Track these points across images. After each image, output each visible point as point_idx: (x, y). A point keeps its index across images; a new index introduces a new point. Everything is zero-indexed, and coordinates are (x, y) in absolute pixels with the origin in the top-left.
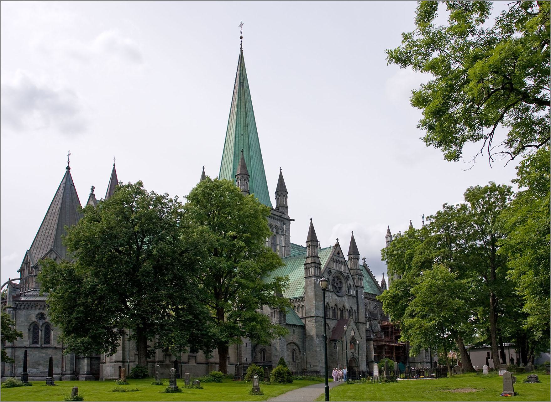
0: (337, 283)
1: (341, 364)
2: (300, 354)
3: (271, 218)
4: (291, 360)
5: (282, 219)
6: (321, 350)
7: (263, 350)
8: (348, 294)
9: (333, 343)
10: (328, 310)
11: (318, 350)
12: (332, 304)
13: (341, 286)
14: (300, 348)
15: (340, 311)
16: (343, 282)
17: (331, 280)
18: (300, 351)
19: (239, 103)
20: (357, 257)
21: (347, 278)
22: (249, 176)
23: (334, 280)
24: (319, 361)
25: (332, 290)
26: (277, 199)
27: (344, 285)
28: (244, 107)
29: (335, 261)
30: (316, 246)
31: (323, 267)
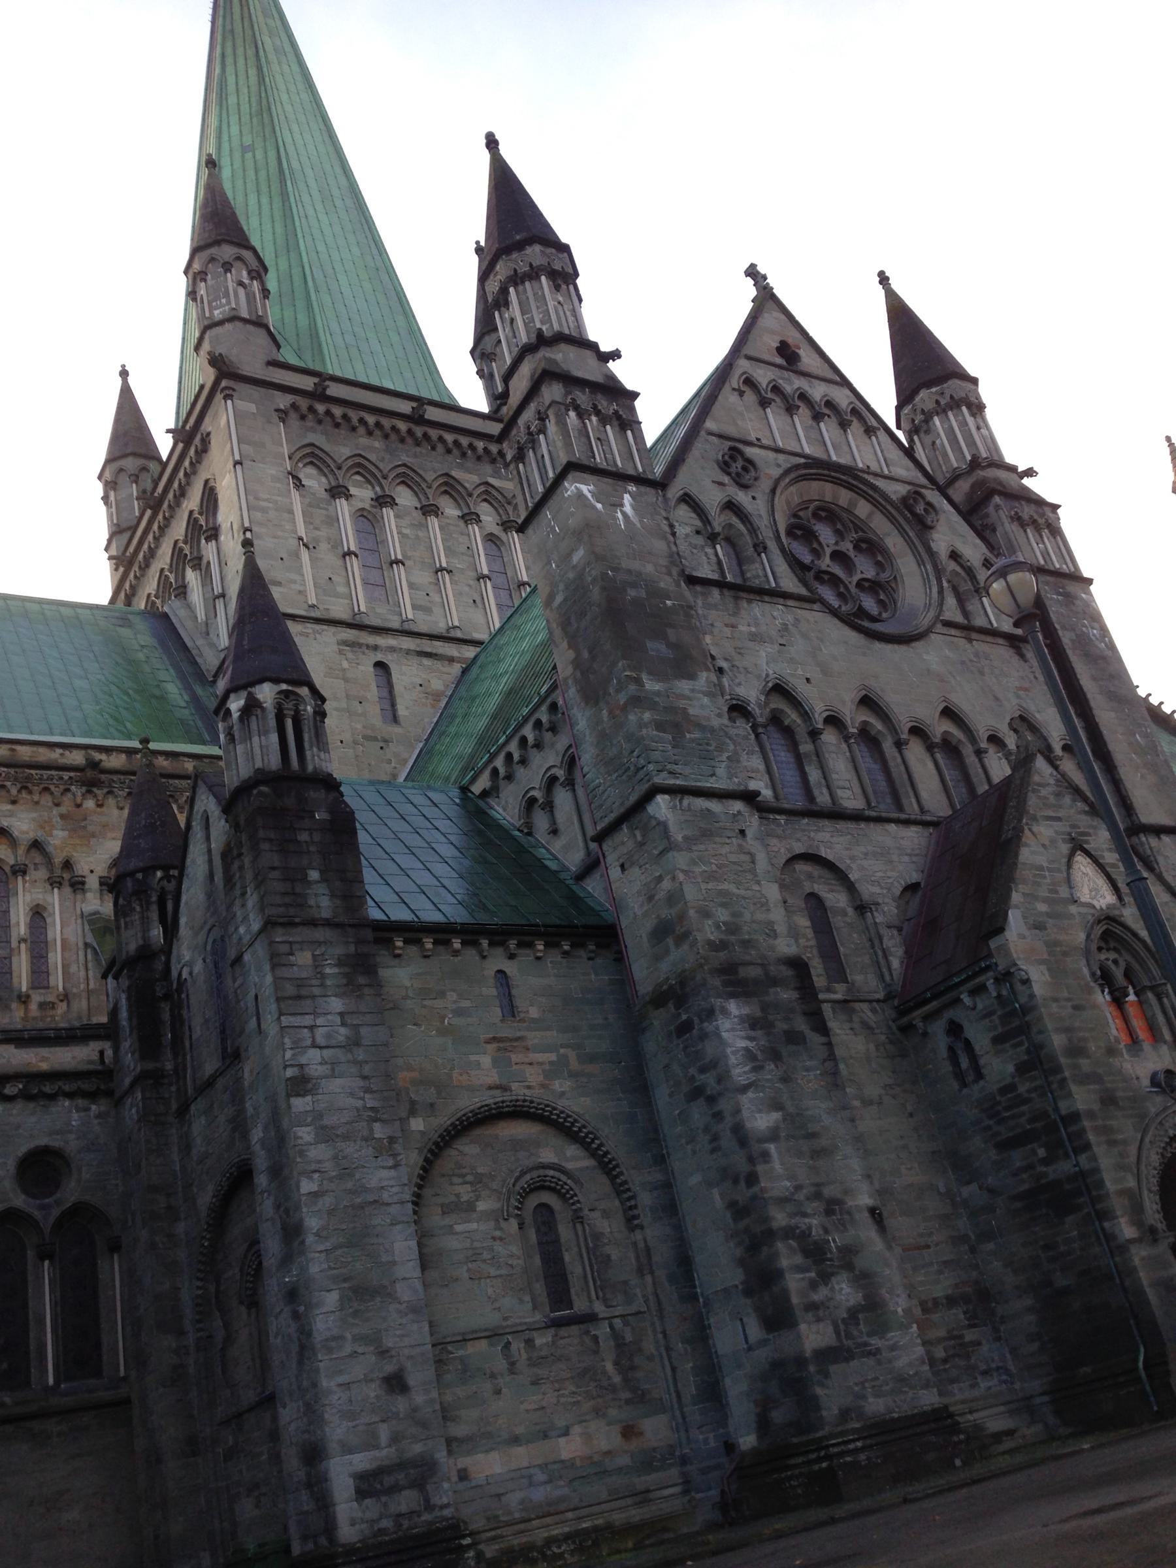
0: (839, 556)
2: (631, 1222)
8: (959, 618)
9: (938, 1028)
10: (806, 747)
13: (884, 576)
14: (614, 1141)
15: (930, 748)
16: (893, 542)
18: (620, 1189)
19: (229, 51)
27: (907, 565)
28: (251, 52)
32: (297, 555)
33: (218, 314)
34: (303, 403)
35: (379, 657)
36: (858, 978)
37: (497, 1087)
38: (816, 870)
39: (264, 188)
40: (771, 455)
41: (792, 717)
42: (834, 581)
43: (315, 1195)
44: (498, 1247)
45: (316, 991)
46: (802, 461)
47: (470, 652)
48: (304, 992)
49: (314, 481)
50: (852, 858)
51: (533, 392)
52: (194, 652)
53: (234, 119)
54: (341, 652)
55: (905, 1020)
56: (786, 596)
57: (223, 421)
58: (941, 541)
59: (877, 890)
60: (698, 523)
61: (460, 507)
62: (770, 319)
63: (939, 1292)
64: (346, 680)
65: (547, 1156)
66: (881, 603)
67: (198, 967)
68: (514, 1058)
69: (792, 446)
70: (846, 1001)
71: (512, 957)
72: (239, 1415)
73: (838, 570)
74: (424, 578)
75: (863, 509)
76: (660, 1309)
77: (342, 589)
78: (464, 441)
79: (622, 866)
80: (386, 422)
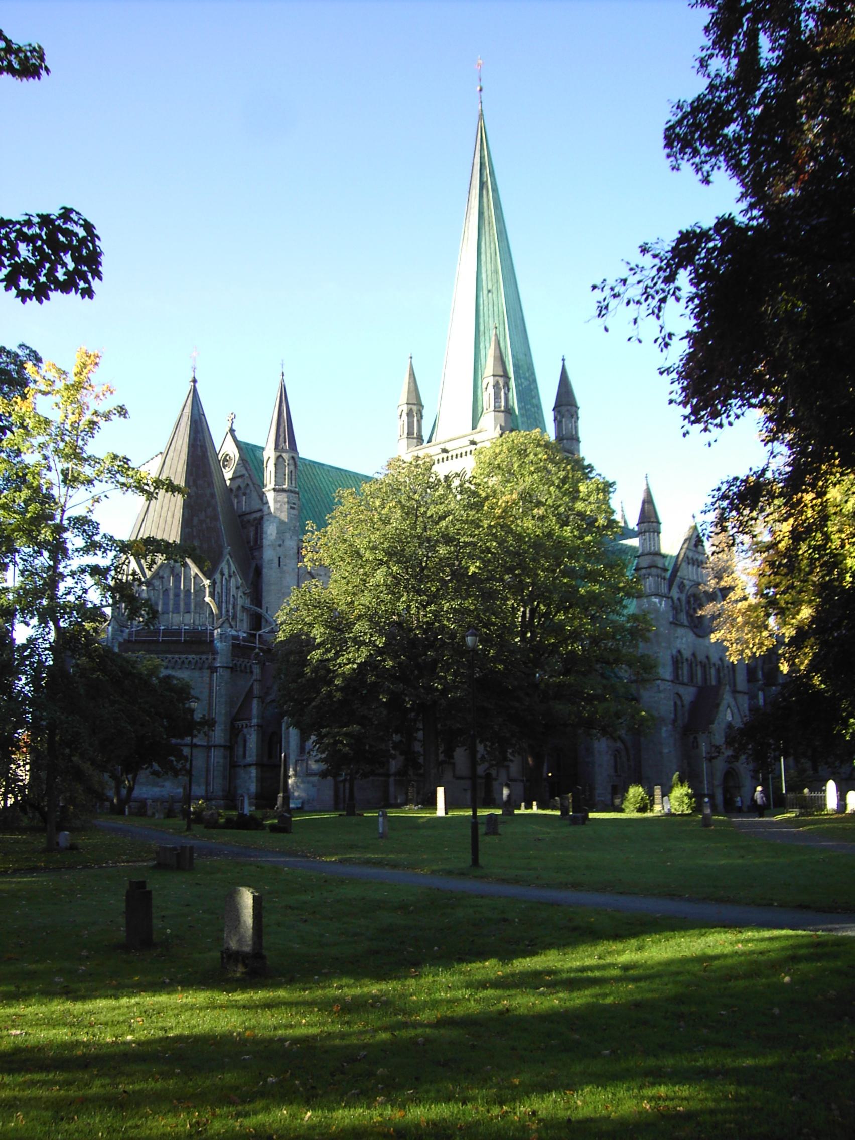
6: (670, 751)
10: (680, 665)
11: (666, 751)
12: (687, 654)
15: (702, 666)
17: (684, 602)
23: (689, 602)
29: (691, 561)
56: (685, 626)
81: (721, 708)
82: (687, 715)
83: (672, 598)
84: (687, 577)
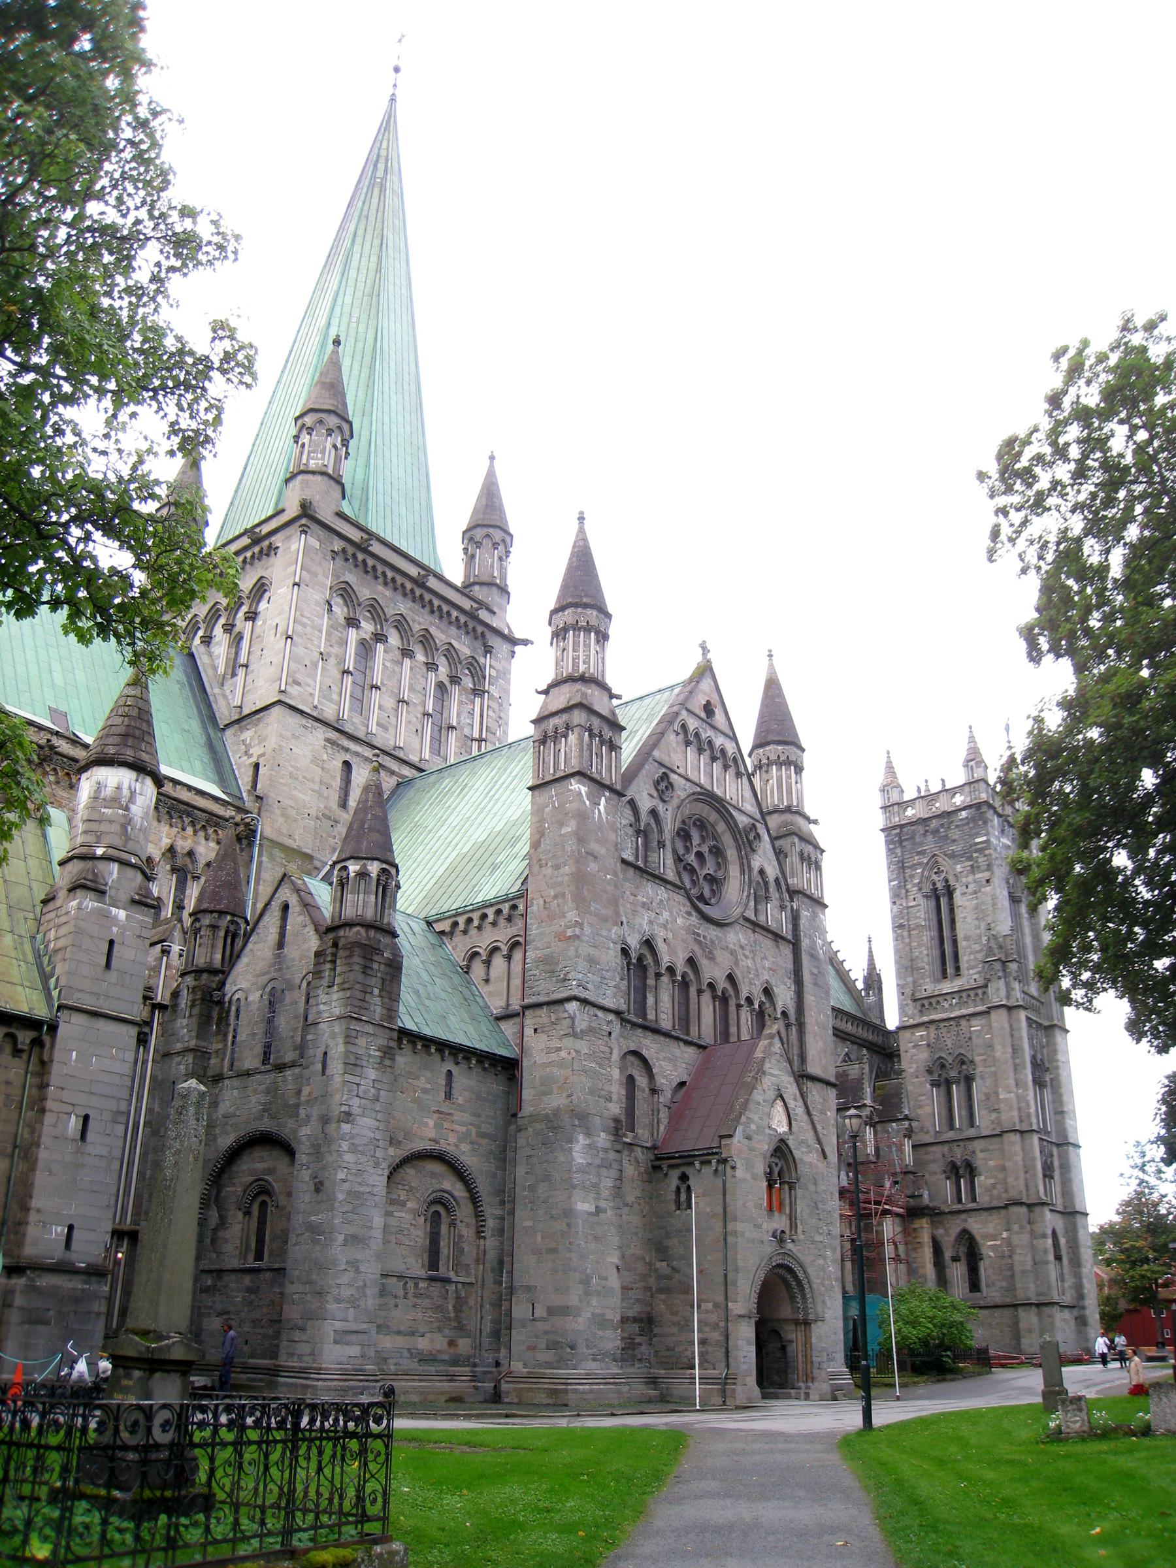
0: (699, 855)
1: (716, 1306)
2: (479, 1234)
3: (432, 612)
4: (418, 1269)
5: (480, 629)
6: (599, 1210)
7: (262, 1192)
8: (753, 918)
9: (675, 1175)
10: (651, 982)
11: (584, 1206)
12: (673, 954)
13: (720, 874)
14: (484, 1187)
15: (714, 997)
16: (731, 853)
18: (478, 1214)
19: (360, 232)
20: (792, 758)
21: (747, 840)
22: (350, 424)
23: (683, 834)
24: (586, 1281)
25: (671, 875)
26: (470, 558)
27: (734, 871)
28: (377, 242)
30: (597, 633)
31: (629, 748)
32: (316, 666)
33: (313, 465)
34: (350, 550)
35: (348, 757)
36: (640, 1131)
37: (434, 1140)
38: (636, 1062)
39: (358, 357)
40: (683, 781)
41: (649, 960)
42: (692, 871)
43: (344, 1181)
44: (412, 1229)
45: (365, 1063)
46: (699, 789)
47: (407, 772)
48: (358, 1062)
49: (340, 611)
50: (658, 1059)
51: (568, 709)
52: (211, 698)
53: (350, 290)
54: (325, 747)
55: (658, 1163)
56: (666, 882)
57: (294, 547)
58: (757, 862)
59: (664, 1081)
60: (633, 819)
61: (427, 655)
62: (706, 684)
63: (630, 1314)
64: (323, 769)
65: (446, 1185)
66: (713, 891)
67: (254, 997)
68: (446, 1125)
69: (695, 778)
70: (631, 1144)
71: (457, 1064)
72: (221, 1271)
73: (695, 865)
74: (390, 703)
75: (721, 827)
76: (483, 1285)
77: (335, 697)
78: (445, 608)
79: (536, 1030)
80: (400, 579)
81: (758, 1096)
82: (664, 1115)
83: (632, 803)
84: (681, 771)
